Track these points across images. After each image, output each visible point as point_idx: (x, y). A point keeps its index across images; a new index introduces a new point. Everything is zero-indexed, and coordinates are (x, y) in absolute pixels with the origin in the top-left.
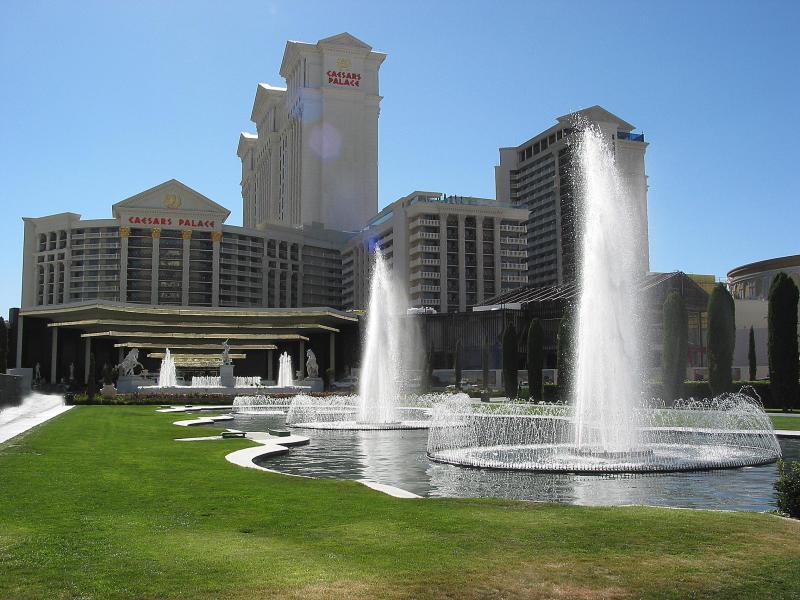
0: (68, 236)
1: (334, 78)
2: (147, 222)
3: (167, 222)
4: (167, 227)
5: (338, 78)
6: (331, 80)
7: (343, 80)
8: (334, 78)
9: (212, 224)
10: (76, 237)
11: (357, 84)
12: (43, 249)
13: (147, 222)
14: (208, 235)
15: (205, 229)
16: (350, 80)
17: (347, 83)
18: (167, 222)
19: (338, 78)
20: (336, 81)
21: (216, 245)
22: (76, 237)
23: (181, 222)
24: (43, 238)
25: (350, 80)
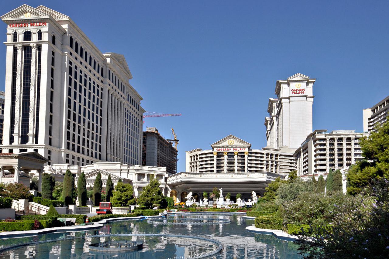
0: (198, 156)
1: (294, 92)
2: (223, 150)
3: (229, 150)
4: (229, 151)
5: (296, 92)
6: (293, 93)
7: (298, 92)
8: (294, 92)
9: (245, 149)
10: (201, 156)
11: (303, 93)
12: (191, 160)
13: (223, 150)
14: (244, 153)
15: (242, 151)
16: (300, 92)
17: (299, 93)
18: (229, 150)
19: (296, 92)
20: (295, 93)
21: (246, 156)
22: (201, 156)
23: (234, 149)
24: (191, 157)
25: (300, 92)
